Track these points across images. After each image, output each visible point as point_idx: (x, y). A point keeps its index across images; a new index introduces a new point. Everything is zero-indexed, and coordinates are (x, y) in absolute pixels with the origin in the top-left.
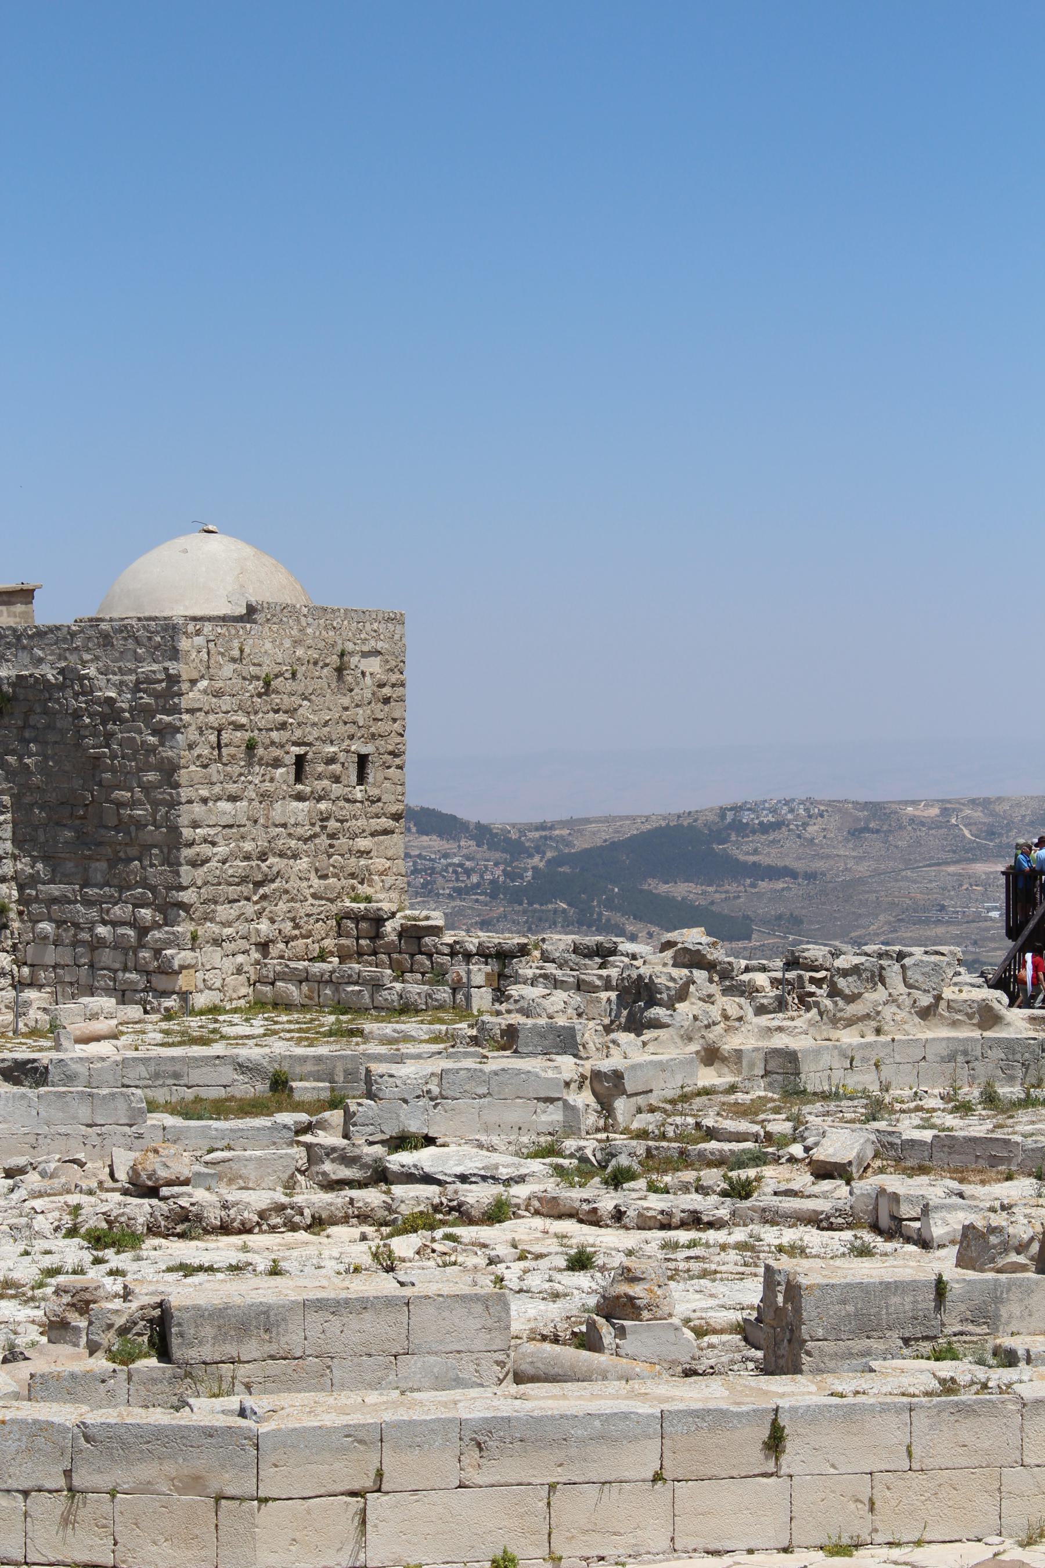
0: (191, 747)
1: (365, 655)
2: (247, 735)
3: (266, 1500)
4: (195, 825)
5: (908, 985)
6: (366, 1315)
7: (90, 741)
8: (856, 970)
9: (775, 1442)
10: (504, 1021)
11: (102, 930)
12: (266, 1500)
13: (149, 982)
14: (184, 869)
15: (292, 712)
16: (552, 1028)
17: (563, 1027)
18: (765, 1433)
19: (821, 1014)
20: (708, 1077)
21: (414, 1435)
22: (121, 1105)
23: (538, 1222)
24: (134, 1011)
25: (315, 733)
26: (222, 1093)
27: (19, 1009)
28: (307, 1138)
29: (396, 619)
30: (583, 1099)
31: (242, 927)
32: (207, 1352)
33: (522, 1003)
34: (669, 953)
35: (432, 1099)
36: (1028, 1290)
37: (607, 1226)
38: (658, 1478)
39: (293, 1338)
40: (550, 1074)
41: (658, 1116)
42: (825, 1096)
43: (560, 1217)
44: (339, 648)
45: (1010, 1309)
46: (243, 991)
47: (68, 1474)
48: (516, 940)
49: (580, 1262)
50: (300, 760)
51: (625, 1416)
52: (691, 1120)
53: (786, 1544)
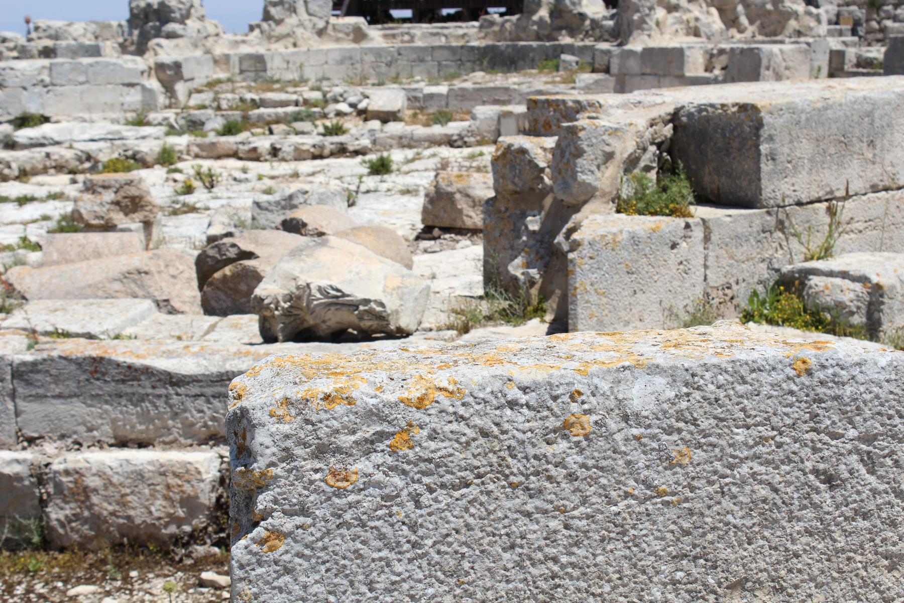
5: (310, 14)
17: (90, 46)
19: (262, 32)
30: (153, 84)
32: (802, 184)
33: (53, 32)
35: (45, 86)
37: (266, 160)
43: (219, 157)
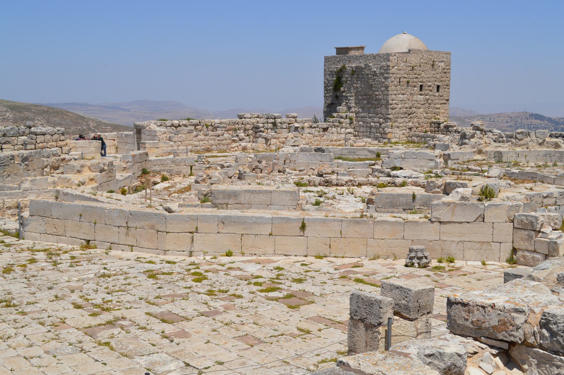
0: (392, 82)
1: (440, 62)
2: (407, 80)
3: (168, 232)
4: (393, 100)
6: (260, 195)
7: (370, 81)
8: (522, 133)
9: (303, 227)
10: (434, 143)
11: (372, 124)
12: (168, 232)
13: (381, 135)
14: (389, 110)
15: (419, 75)
16: (444, 144)
18: (300, 225)
21: (206, 219)
22: (328, 157)
24: (376, 142)
25: (426, 80)
26: (365, 157)
31: (405, 124)
32: (221, 201)
38: (270, 235)
39: (242, 199)
40: (432, 154)
44: (433, 60)
46: (405, 139)
47: (127, 223)
50: (421, 86)
51: (262, 218)
52: (466, 166)
53: (306, 254)
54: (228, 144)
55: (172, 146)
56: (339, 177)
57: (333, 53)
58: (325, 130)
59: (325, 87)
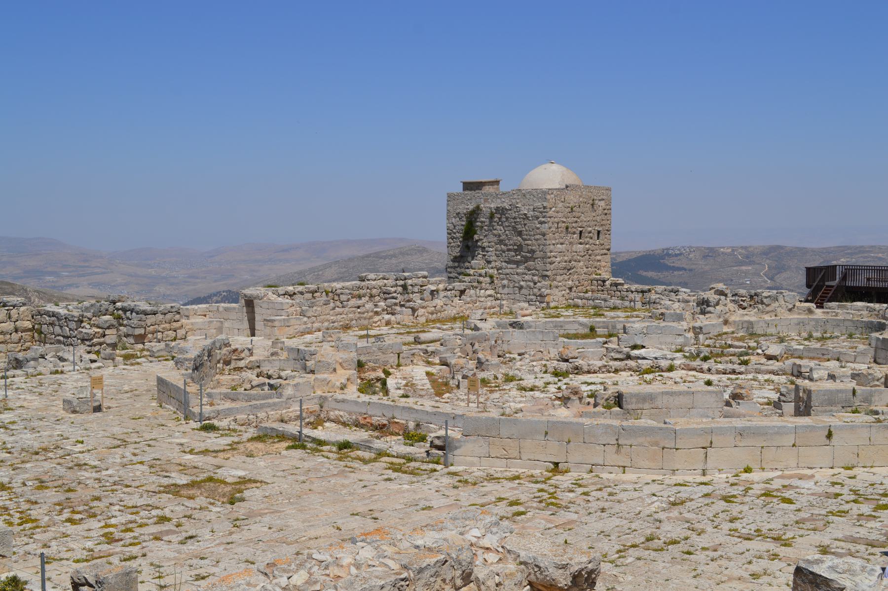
1: (600, 200)
9: (829, 436)
10: (660, 311)
15: (578, 218)
16: (676, 313)
18: (826, 433)
20: (726, 329)
21: (721, 431)
22: (551, 335)
23: (684, 372)
24: (533, 308)
26: (575, 332)
27: (501, 306)
28: (606, 345)
29: (609, 189)
30: (690, 335)
32: (633, 406)
34: (713, 291)
36: (881, 392)
39: (659, 403)
41: (713, 341)
42: (765, 335)
43: (690, 370)
45: (875, 398)
47: (617, 440)
48: (646, 287)
49: (709, 383)
50: (581, 232)
51: (785, 427)
54: (371, 318)
55: (305, 323)
56: (590, 363)
57: (459, 189)
58: (462, 292)
59: (448, 233)
